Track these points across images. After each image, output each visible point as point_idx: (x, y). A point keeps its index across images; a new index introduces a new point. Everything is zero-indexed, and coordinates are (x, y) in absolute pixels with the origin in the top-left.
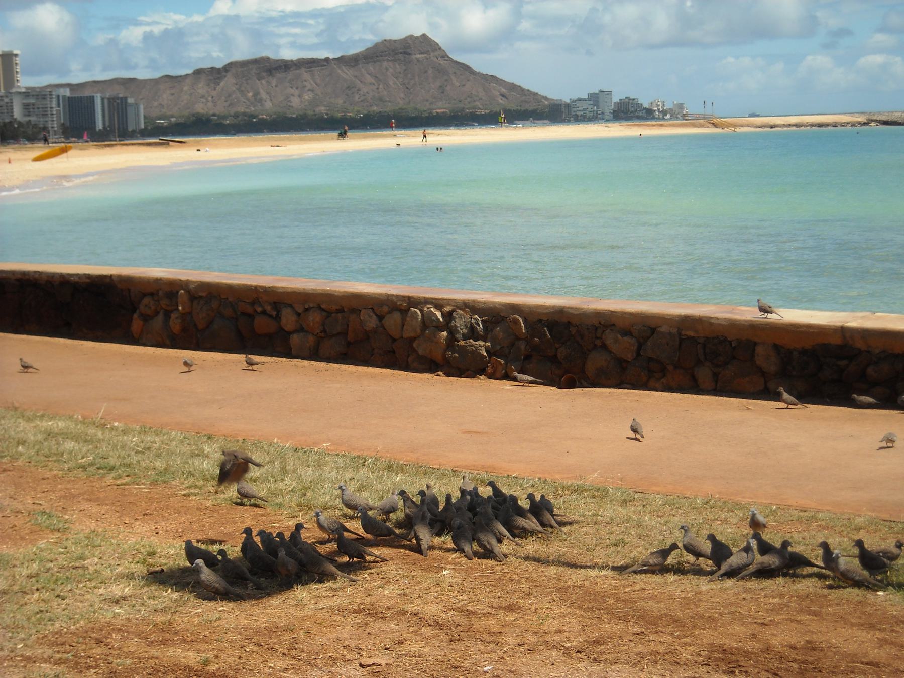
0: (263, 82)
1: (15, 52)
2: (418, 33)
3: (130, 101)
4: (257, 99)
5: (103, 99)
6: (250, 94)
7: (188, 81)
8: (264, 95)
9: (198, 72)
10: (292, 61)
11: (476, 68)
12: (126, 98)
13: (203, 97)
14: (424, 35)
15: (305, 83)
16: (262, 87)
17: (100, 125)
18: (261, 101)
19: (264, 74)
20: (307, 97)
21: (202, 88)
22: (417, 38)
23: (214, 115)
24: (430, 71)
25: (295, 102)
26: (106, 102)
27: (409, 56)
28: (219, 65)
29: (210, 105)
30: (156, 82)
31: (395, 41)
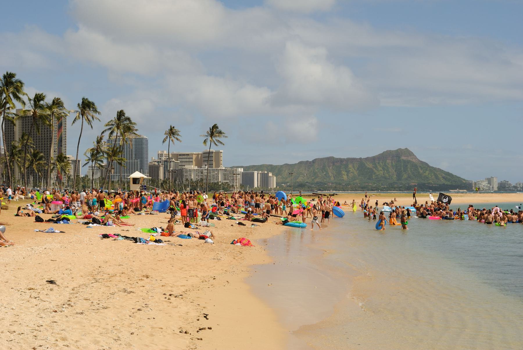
0: (331, 168)
1: (221, 151)
2: (403, 148)
3: (270, 174)
5: (258, 174)
8: (330, 174)
9: (301, 163)
11: (431, 165)
12: (268, 174)
14: (406, 149)
15: (351, 170)
17: (256, 186)
20: (351, 175)
22: (403, 150)
23: (307, 182)
25: (345, 177)
28: (311, 160)
30: (281, 166)
31: (392, 151)
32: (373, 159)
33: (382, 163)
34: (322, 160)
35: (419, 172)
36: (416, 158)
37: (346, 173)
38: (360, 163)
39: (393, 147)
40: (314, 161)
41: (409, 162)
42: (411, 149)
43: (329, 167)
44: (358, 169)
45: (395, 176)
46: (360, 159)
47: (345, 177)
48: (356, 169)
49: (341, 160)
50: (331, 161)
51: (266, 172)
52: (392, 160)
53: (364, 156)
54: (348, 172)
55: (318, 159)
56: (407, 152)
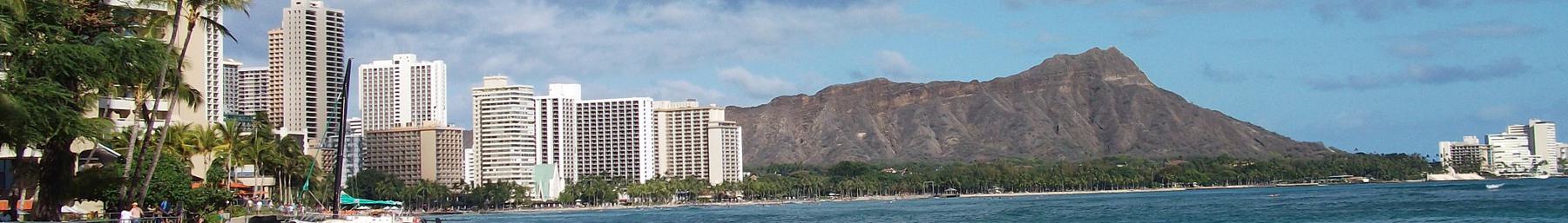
0: (879, 117)
2: (1104, 47)
4: (872, 142)
6: (861, 135)
7: (764, 116)
9: (780, 102)
10: (922, 85)
12: (706, 111)
13: (788, 139)
14: (1113, 49)
16: (878, 122)
17: (646, 174)
18: (878, 145)
19: (881, 104)
20: (952, 140)
21: (785, 126)
24: (1135, 104)
25: (934, 145)
26: (662, 117)
27: (1096, 81)
29: (799, 151)
32: (1013, 86)
33: (1044, 95)
34: (847, 90)
35: (1173, 123)
36: (1143, 77)
37: (933, 134)
38: (978, 99)
39: (1077, 49)
40: (822, 96)
41: (1132, 89)
42: (1125, 51)
43: (874, 112)
44: (971, 117)
45: (1095, 139)
46: (975, 82)
47: (934, 145)
48: (964, 117)
49: (914, 89)
50: (880, 91)
51: (695, 105)
52: (1075, 86)
53: (985, 76)
54: (939, 129)
55: (836, 87)
56: (1115, 60)
